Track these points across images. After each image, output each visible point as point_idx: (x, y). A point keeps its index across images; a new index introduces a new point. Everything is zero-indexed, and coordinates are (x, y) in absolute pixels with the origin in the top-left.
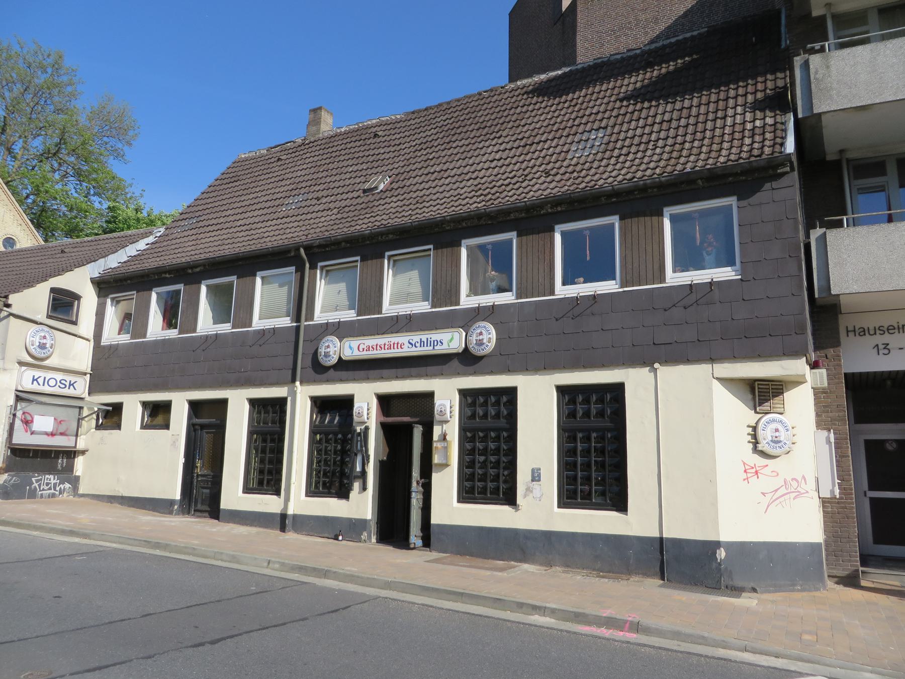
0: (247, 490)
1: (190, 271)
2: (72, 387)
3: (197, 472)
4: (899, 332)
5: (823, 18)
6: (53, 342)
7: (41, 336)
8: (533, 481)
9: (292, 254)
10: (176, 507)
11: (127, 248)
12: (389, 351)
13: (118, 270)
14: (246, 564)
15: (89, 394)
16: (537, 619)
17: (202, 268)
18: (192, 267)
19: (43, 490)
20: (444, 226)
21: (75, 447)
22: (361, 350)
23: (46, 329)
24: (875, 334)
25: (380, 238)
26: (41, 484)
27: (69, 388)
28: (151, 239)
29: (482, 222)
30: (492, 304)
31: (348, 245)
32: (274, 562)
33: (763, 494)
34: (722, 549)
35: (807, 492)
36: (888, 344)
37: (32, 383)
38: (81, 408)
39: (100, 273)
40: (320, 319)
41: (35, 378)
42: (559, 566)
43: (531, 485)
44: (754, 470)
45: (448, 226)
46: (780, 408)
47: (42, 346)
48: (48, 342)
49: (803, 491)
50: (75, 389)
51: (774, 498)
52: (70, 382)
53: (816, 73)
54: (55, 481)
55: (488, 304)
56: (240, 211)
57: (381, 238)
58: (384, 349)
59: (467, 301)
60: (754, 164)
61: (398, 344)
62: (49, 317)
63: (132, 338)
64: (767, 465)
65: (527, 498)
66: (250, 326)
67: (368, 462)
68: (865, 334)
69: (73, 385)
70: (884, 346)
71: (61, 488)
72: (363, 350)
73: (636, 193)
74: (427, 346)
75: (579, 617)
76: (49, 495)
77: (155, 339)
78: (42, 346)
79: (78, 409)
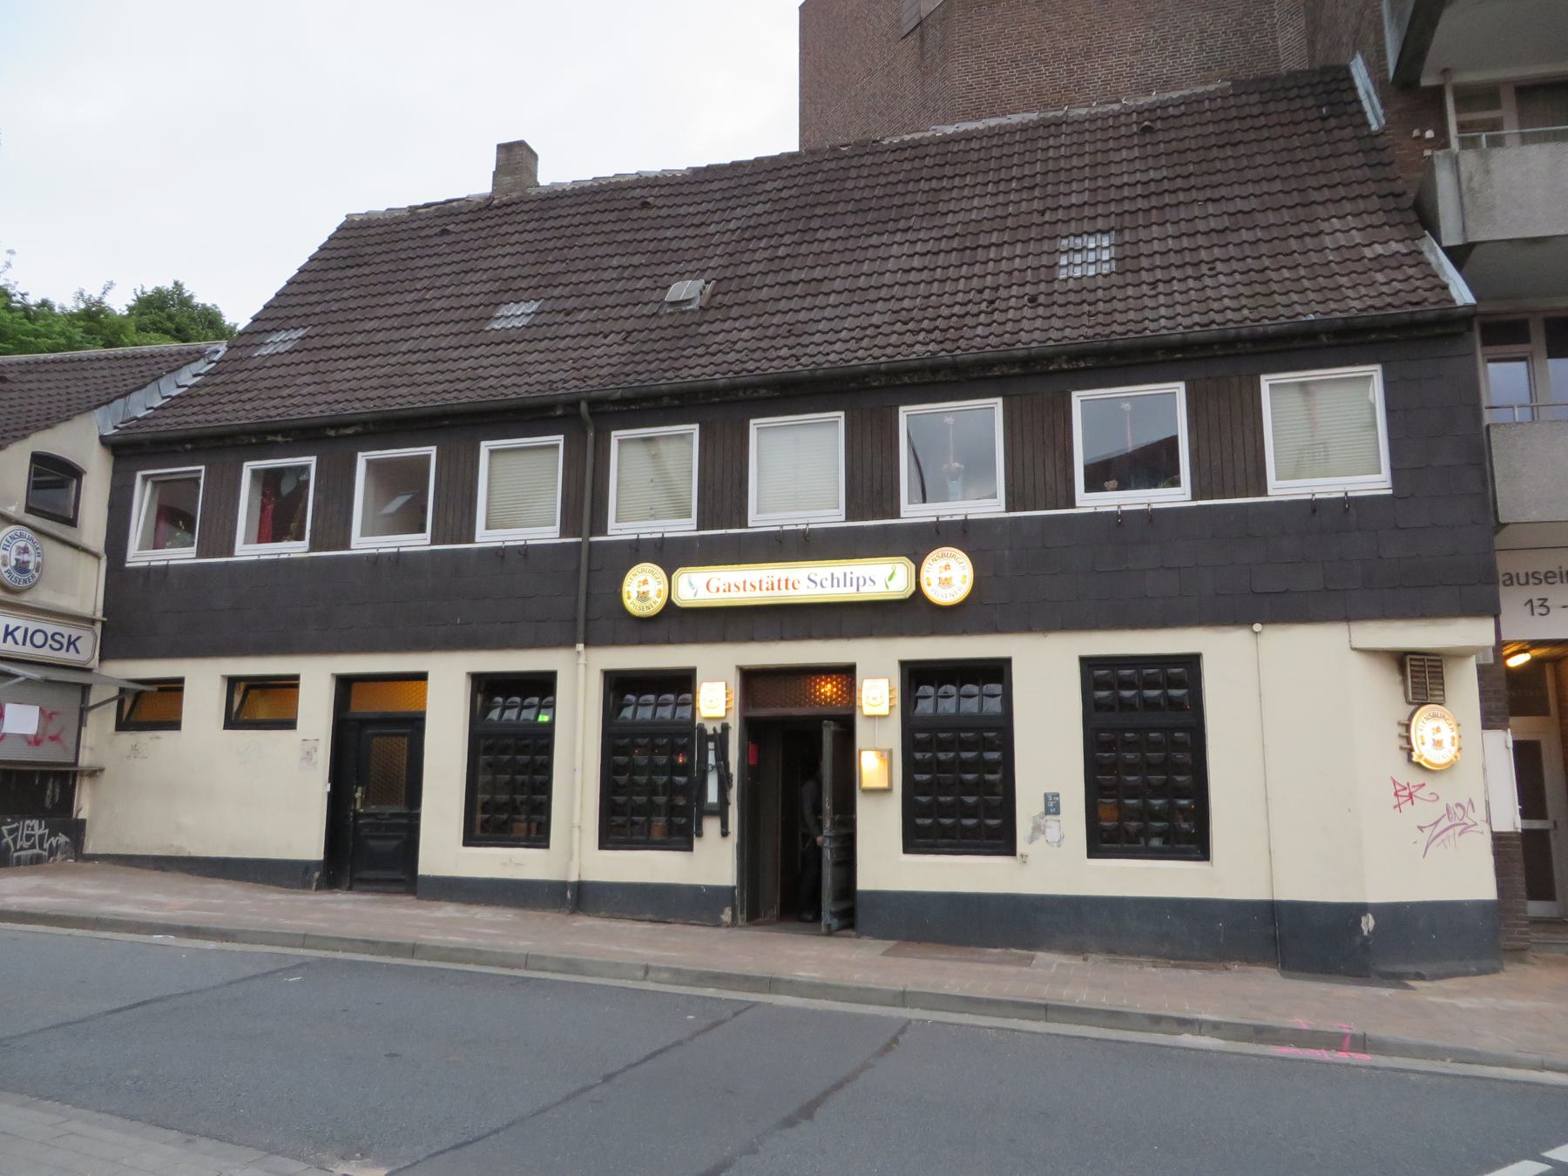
0: (470, 839)
1: (332, 433)
2: (72, 646)
3: (355, 811)
4: (1562, 582)
5: (1437, 93)
6: (39, 559)
7: (19, 548)
8: (1047, 812)
9: (559, 412)
10: (317, 875)
11: (162, 382)
12: (770, 593)
13: (152, 423)
14: (599, 975)
15: (101, 660)
16: (1187, 1039)
17: (360, 429)
18: (333, 426)
19: (22, 849)
20: (867, 380)
21: (76, 763)
22: (713, 587)
23: (28, 533)
24: (1527, 583)
25: (741, 394)
26: (17, 837)
27: (68, 650)
28: (202, 367)
29: (940, 377)
30: (962, 518)
31: (676, 402)
32: (659, 969)
33: (1421, 828)
34: (1370, 916)
35: (1476, 824)
36: (1545, 600)
37: (5, 641)
38: (85, 689)
39: (115, 428)
40: (620, 532)
41: (10, 630)
42: (1096, 953)
43: (1042, 822)
44: (1406, 793)
45: (875, 381)
46: (1438, 695)
47: (22, 568)
48: (32, 559)
49: (1470, 823)
50: (77, 652)
51: (1434, 834)
52: (70, 637)
53: (1470, 179)
54: (41, 832)
55: (955, 518)
56: (396, 322)
57: (744, 393)
58: (761, 589)
59: (912, 512)
60: (1419, 317)
61: (787, 580)
62: (29, 510)
63: (199, 555)
64: (1424, 785)
65: (1035, 842)
66: (471, 539)
67: (730, 785)
68: (1512, 584)
69: (74, 643)
70: (1540, 602)
71: (51, 844)
72: (718, 590)
73: (1216, 347)
74: (845, 585)
75: (1261, 1033)
76: (31, 858)
77: (256, 558)
78: (22, 568)
79: (78, 696)
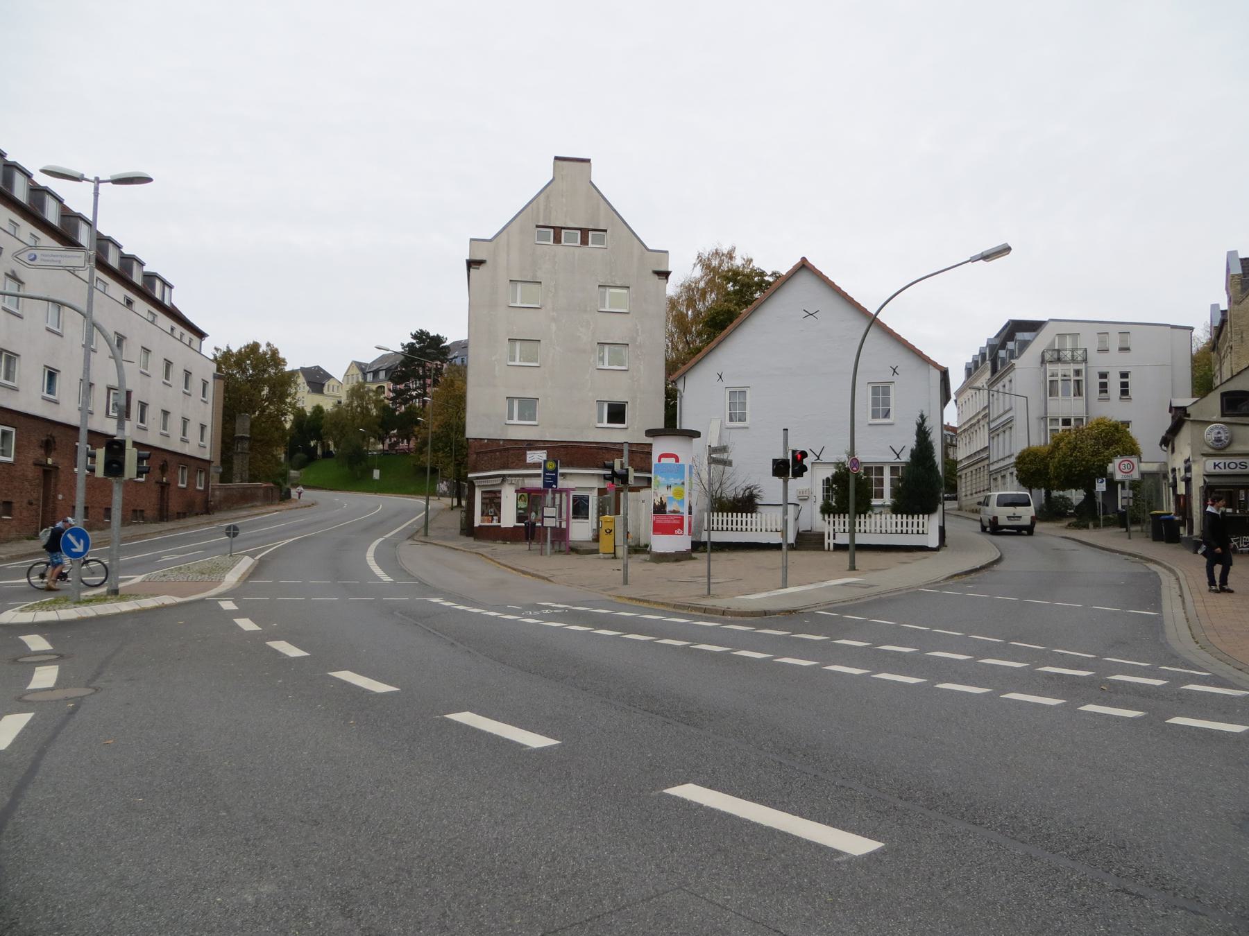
19: (1243, 547)
37: (1215, 468)
